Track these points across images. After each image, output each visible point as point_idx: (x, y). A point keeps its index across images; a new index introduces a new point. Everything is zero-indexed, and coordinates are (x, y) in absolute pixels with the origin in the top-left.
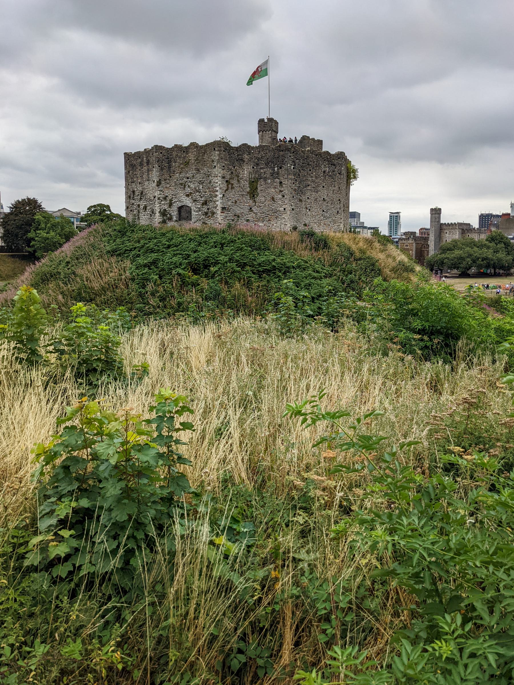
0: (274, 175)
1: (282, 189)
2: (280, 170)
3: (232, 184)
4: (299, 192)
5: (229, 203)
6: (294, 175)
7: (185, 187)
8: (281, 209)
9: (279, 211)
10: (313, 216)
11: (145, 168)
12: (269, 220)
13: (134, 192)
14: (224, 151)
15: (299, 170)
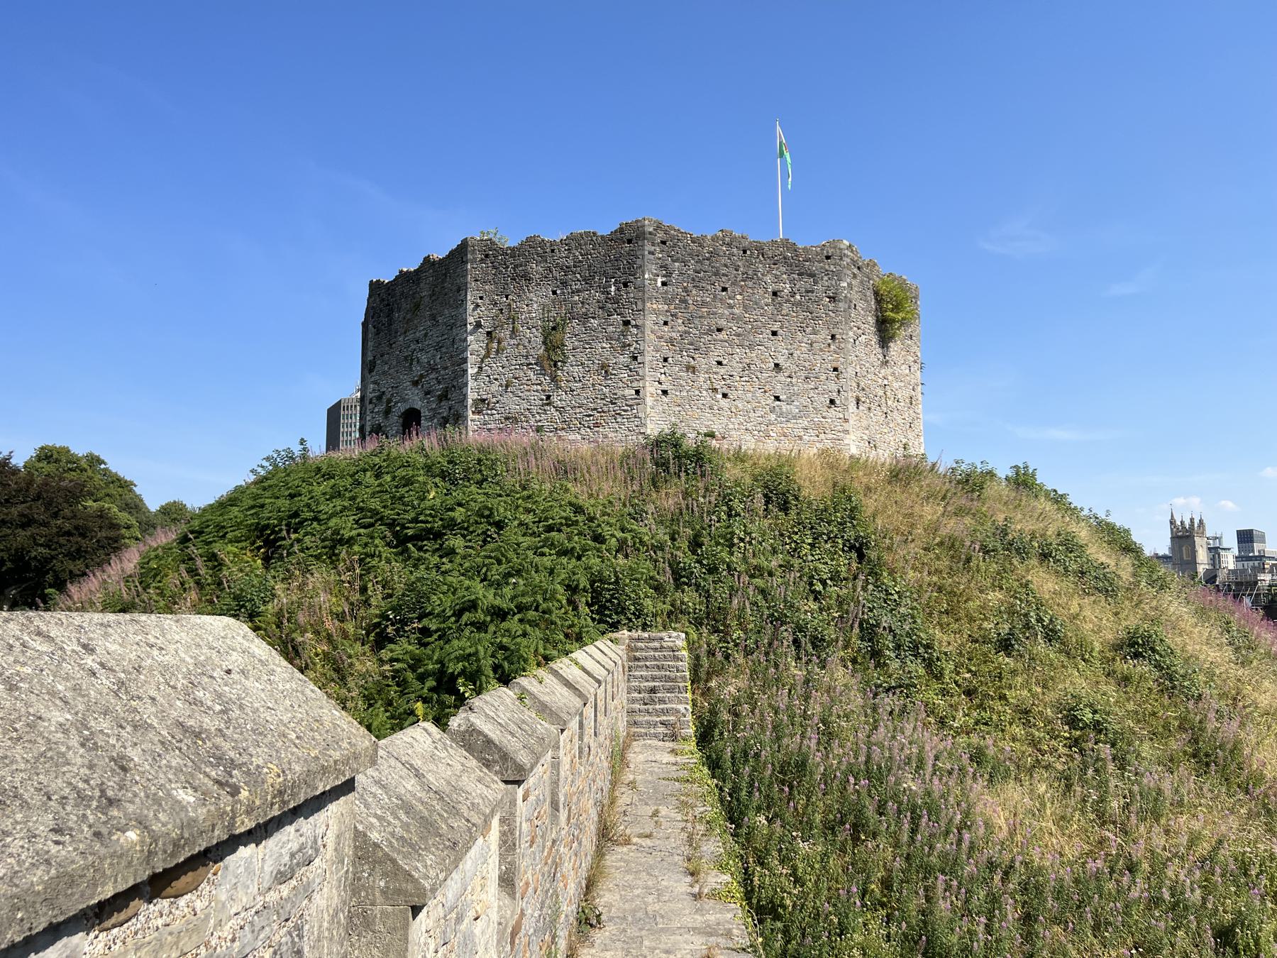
6: (668, 302)
7: (411, 364)
15: (685, 289)
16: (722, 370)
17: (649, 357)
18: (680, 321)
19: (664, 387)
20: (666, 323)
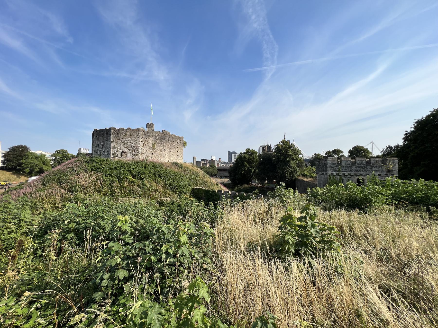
0: (162, 142)
4: (170, 148)
10: (174, 157)
11: (105, 136)
13: (98, 145)
17: (167, 150)
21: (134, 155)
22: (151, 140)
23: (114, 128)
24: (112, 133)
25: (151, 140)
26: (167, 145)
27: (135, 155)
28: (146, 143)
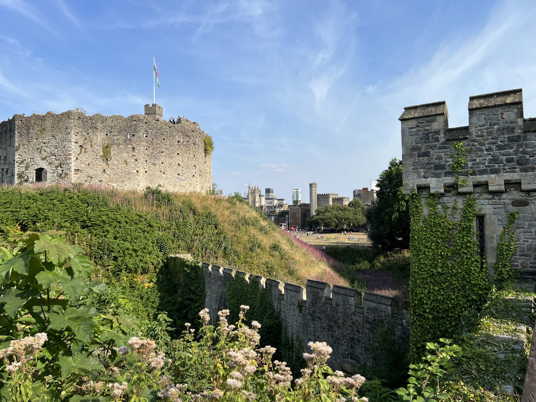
0: (127, 142)
1: (135, 154)
2: (133, 137)
3: (85, 149)
5: (83, 166)
8: (134, 171)
9: (132, 173)
12: (122, 181)
14: (78, 120)
15: (153, 139)
16: (163, 165)
17: (141, 160)
18: (151, 149)
19: (146, 170)
20: (146, 149)
21: (61, 175)
22: (99, 138)
23: (21, 117)
24: (17, 127)
25: (99, 138)
26: (142, 150)
27: (63, 176)
28: (88, 147)
